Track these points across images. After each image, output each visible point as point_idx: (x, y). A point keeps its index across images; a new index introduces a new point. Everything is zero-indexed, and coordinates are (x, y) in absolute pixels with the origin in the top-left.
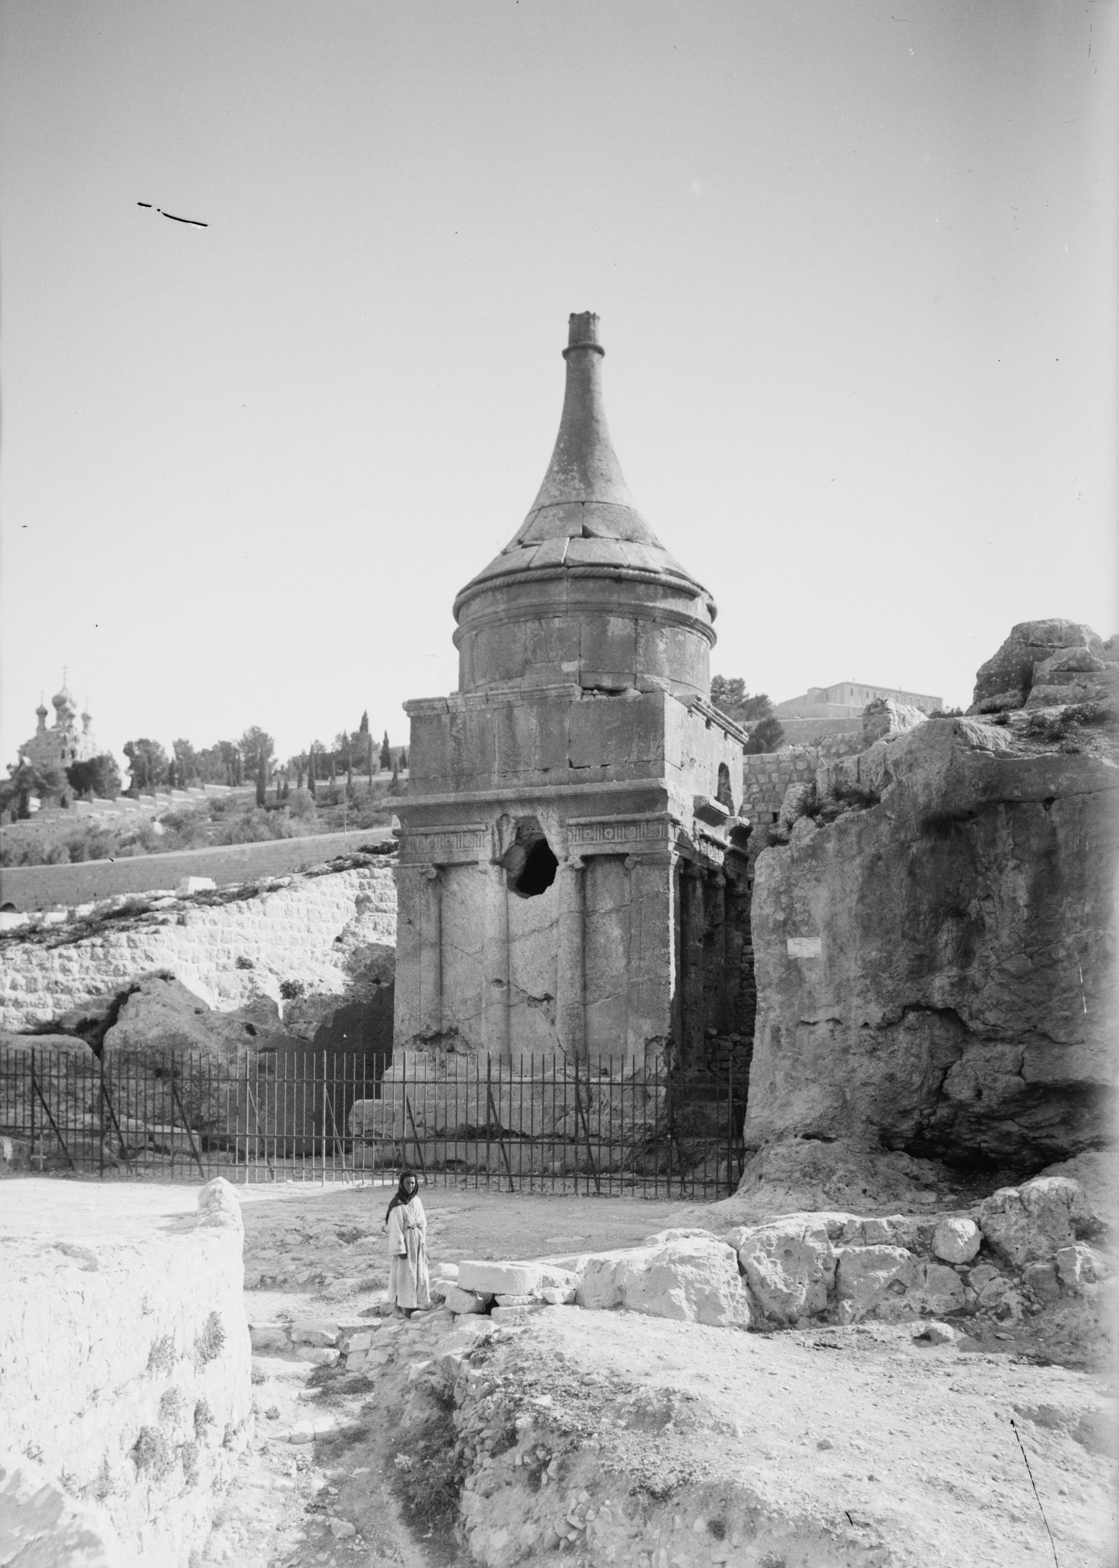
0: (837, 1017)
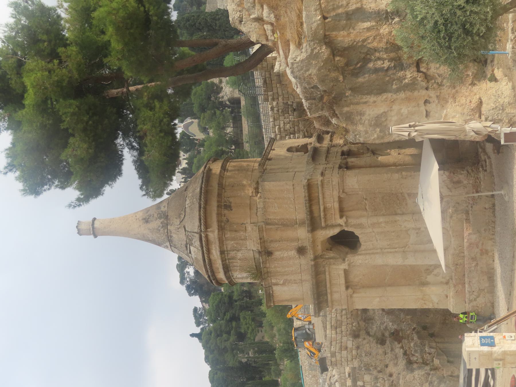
0: (423, 101)
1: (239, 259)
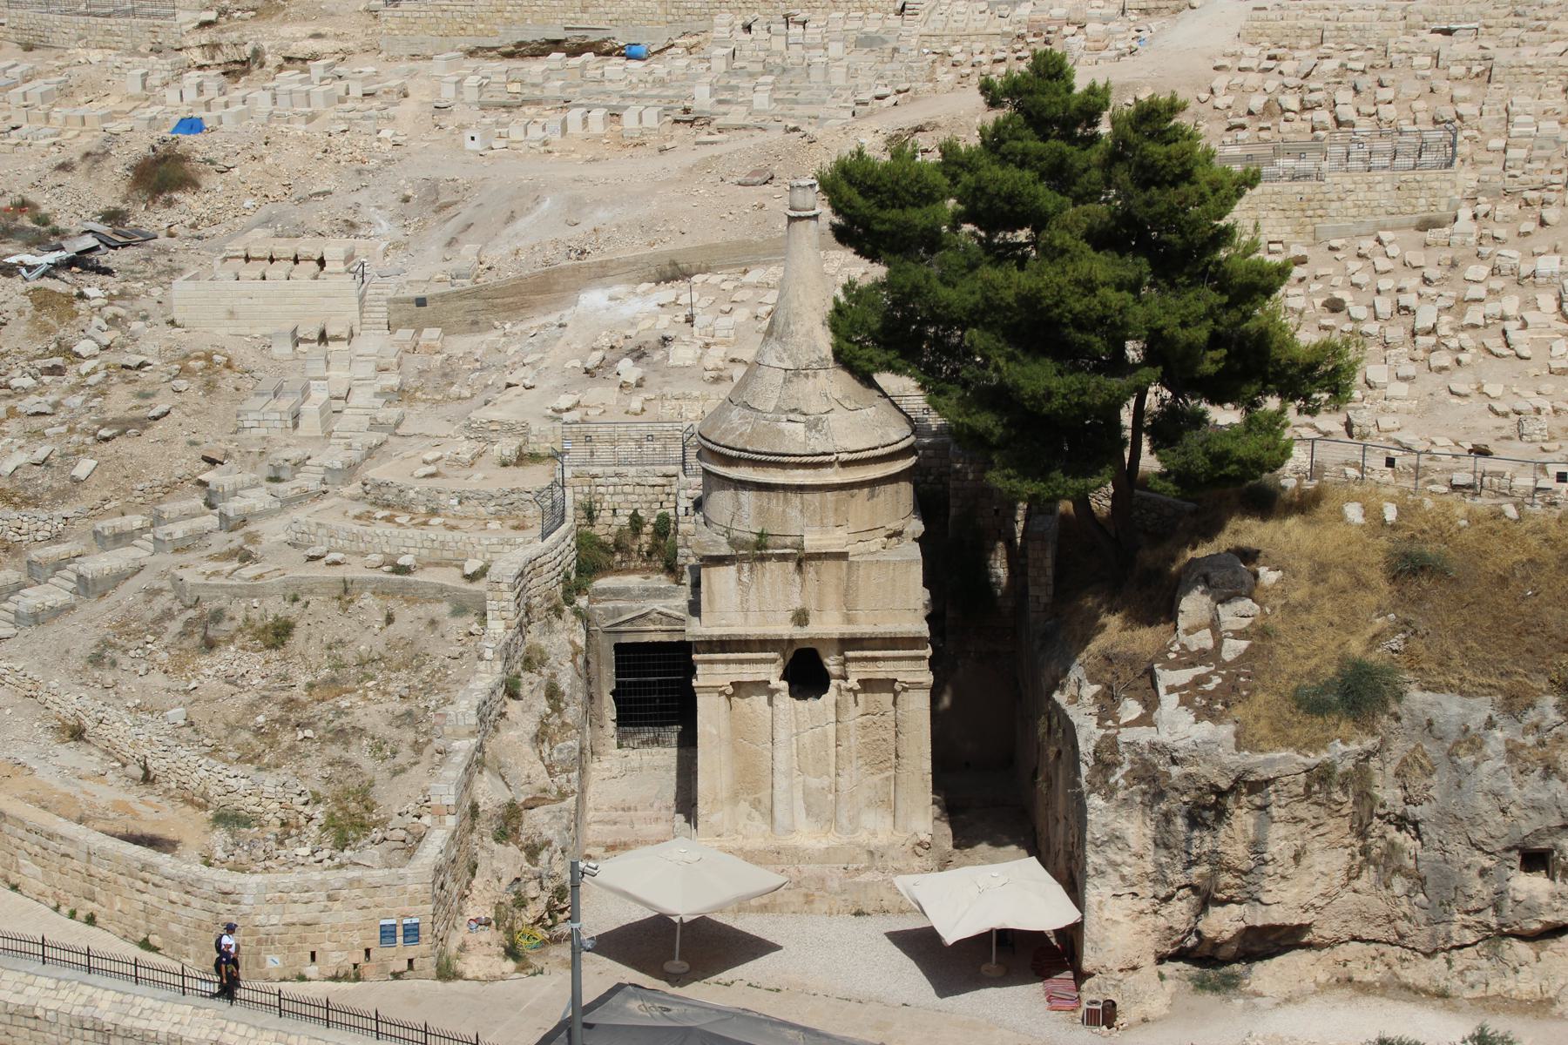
1: (784, 511)
